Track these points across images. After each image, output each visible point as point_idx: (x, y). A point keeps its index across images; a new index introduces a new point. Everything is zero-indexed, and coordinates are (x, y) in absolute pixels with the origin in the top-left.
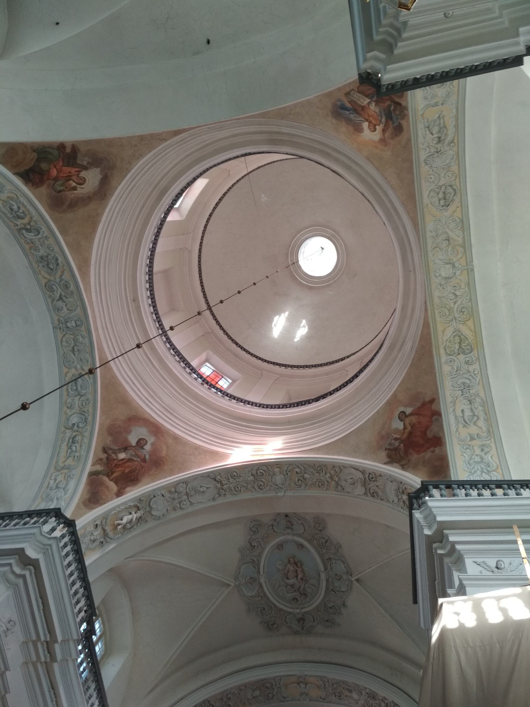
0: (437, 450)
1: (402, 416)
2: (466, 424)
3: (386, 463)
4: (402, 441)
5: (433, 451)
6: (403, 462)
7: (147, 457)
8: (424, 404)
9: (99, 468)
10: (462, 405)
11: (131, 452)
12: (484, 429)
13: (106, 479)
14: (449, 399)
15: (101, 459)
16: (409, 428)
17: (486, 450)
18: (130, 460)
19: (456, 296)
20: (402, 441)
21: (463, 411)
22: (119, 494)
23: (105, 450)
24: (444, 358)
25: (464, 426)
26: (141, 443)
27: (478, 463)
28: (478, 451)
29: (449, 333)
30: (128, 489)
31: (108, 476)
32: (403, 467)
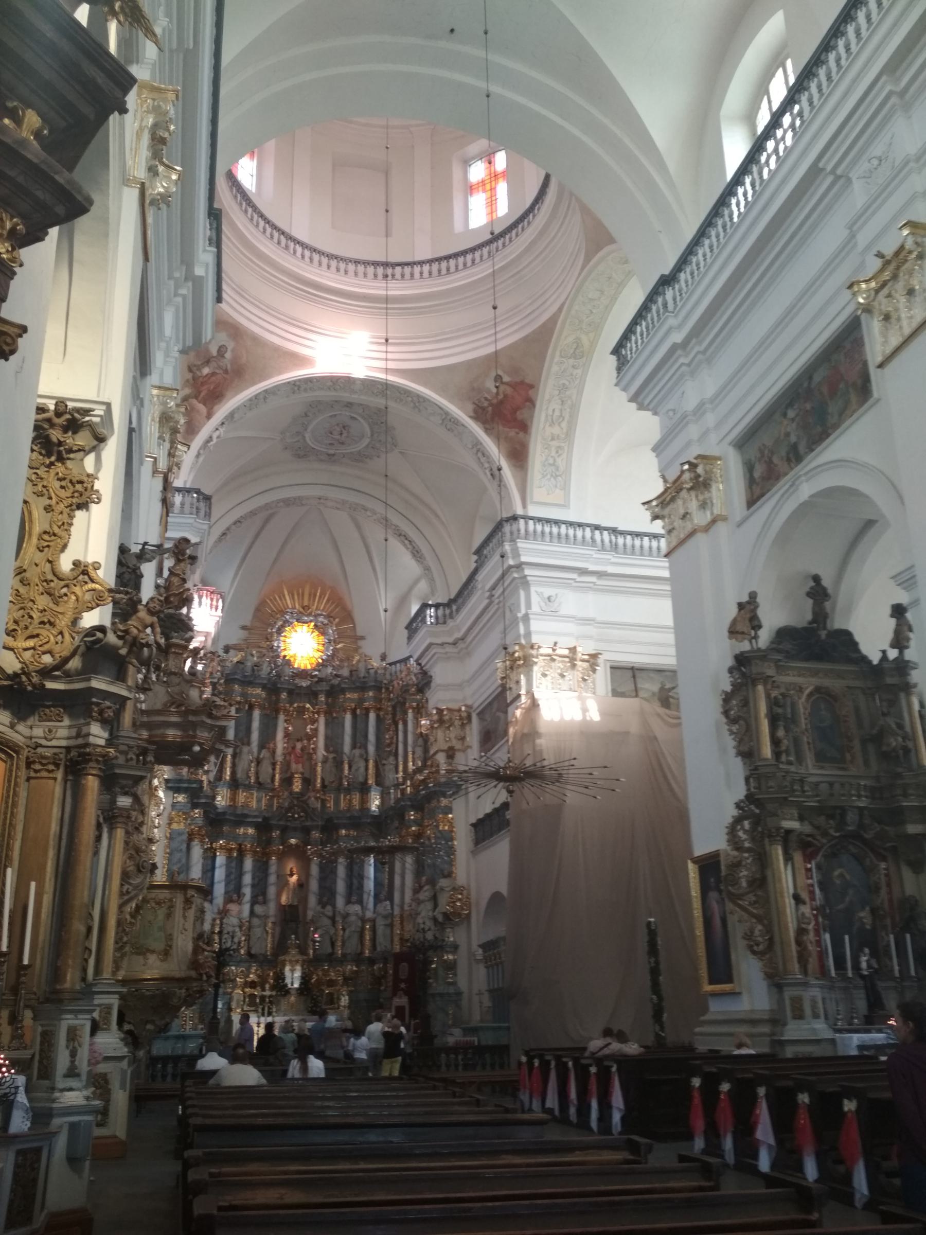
0: (521, 434)
1: (498, 378)
2: (552, 424)
3: (471, 417)
4: (491, 405)
5: (517, 433)
6: (487, 426)
7: (229, 367)
8: (522, 383)
9: (187, 391)
10: (555, 405)
11: (213, 364)
12: (565, 430)
13: (194, 402)
14: (547, 397)
15: (188, 381)
16: (501, 397)
17: (560, 452)
18: (213, 374)
19: (592, 312)
20: (491, 405)
21: (554, 410)
22: (209, 416)
23: (190, 370)
24: (557, 359)
25: (550, 425)
26: (222, 350)
27: (550, 465)
28: (553, 454)
29: (571, 339)
30: (216, 408)
31: (196, 397)
32: (487, 431)
